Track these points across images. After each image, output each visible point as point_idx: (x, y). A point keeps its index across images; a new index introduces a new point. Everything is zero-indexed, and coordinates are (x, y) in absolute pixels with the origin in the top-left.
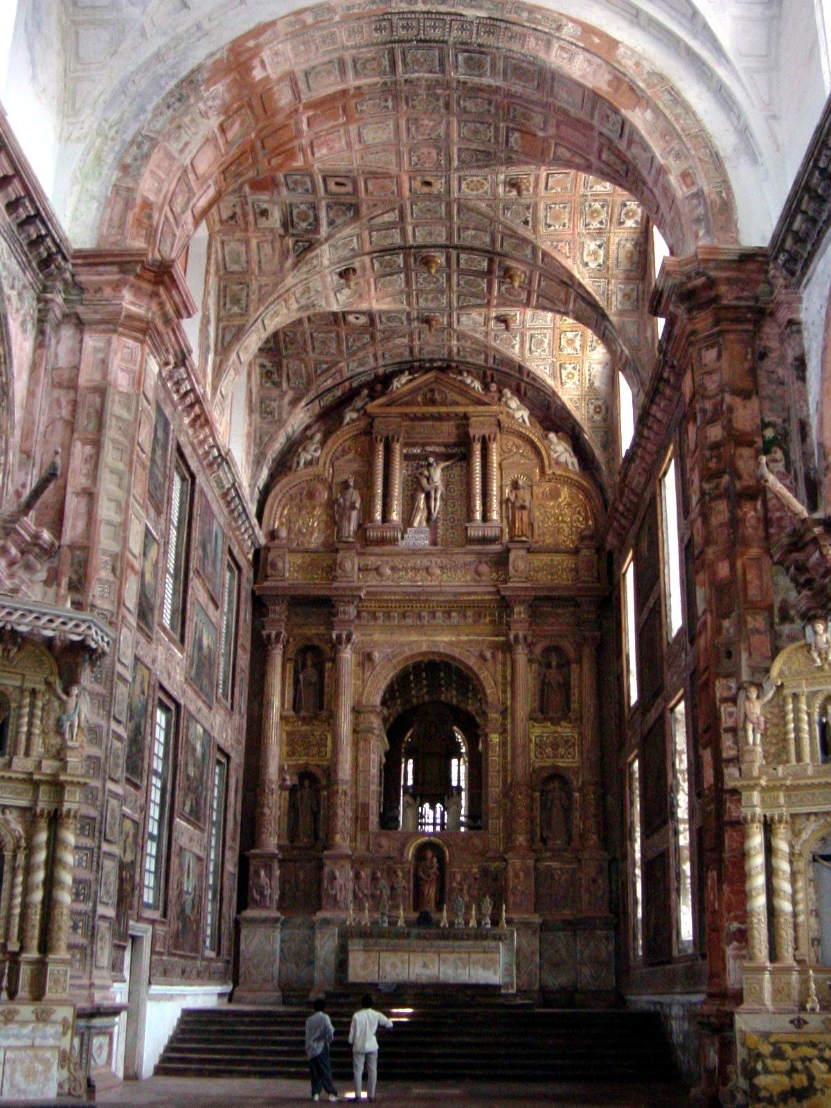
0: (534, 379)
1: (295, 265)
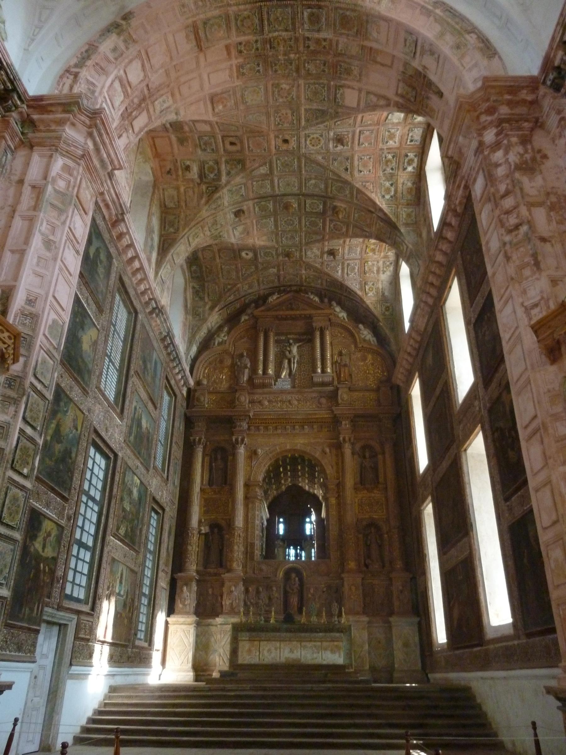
0: (350, 293)
1: (207, 202)
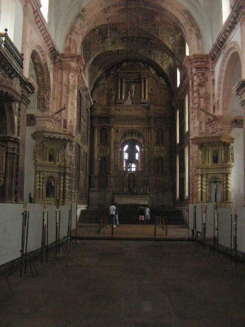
1: (102, 42)
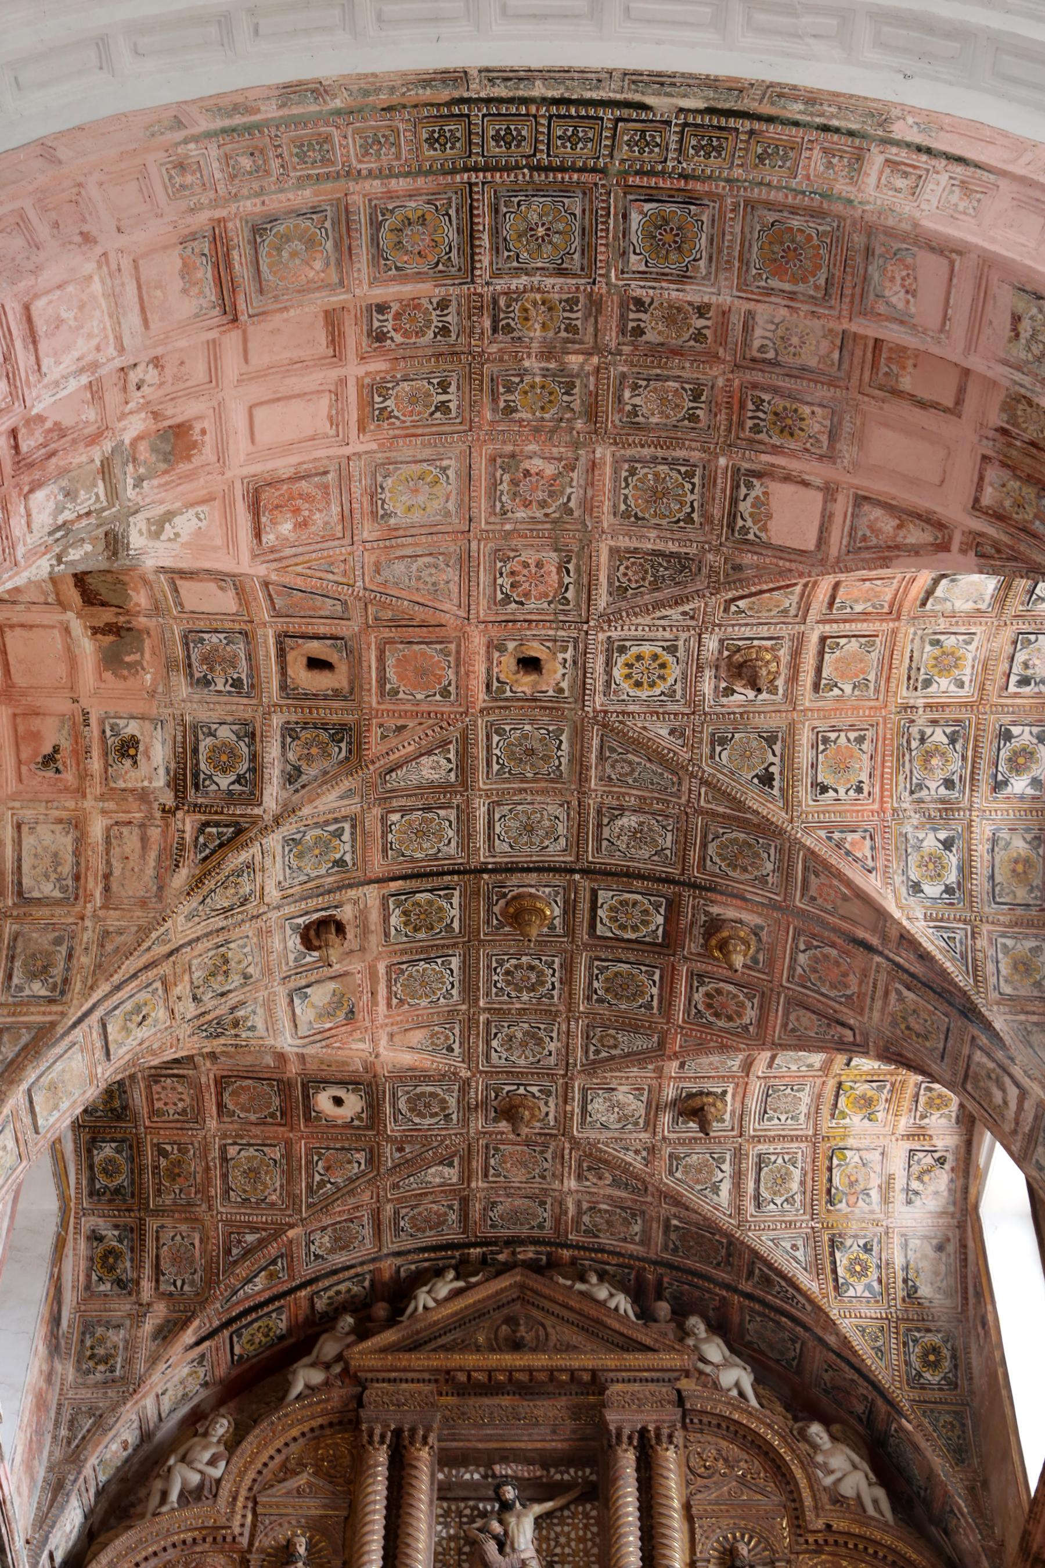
0: (767, 1281)
